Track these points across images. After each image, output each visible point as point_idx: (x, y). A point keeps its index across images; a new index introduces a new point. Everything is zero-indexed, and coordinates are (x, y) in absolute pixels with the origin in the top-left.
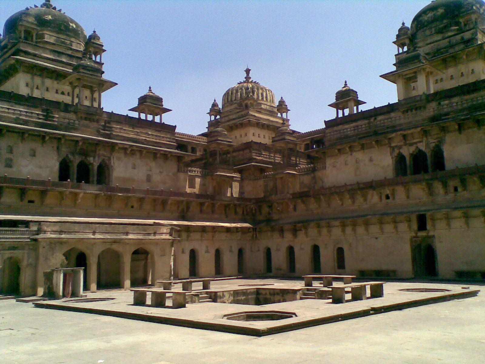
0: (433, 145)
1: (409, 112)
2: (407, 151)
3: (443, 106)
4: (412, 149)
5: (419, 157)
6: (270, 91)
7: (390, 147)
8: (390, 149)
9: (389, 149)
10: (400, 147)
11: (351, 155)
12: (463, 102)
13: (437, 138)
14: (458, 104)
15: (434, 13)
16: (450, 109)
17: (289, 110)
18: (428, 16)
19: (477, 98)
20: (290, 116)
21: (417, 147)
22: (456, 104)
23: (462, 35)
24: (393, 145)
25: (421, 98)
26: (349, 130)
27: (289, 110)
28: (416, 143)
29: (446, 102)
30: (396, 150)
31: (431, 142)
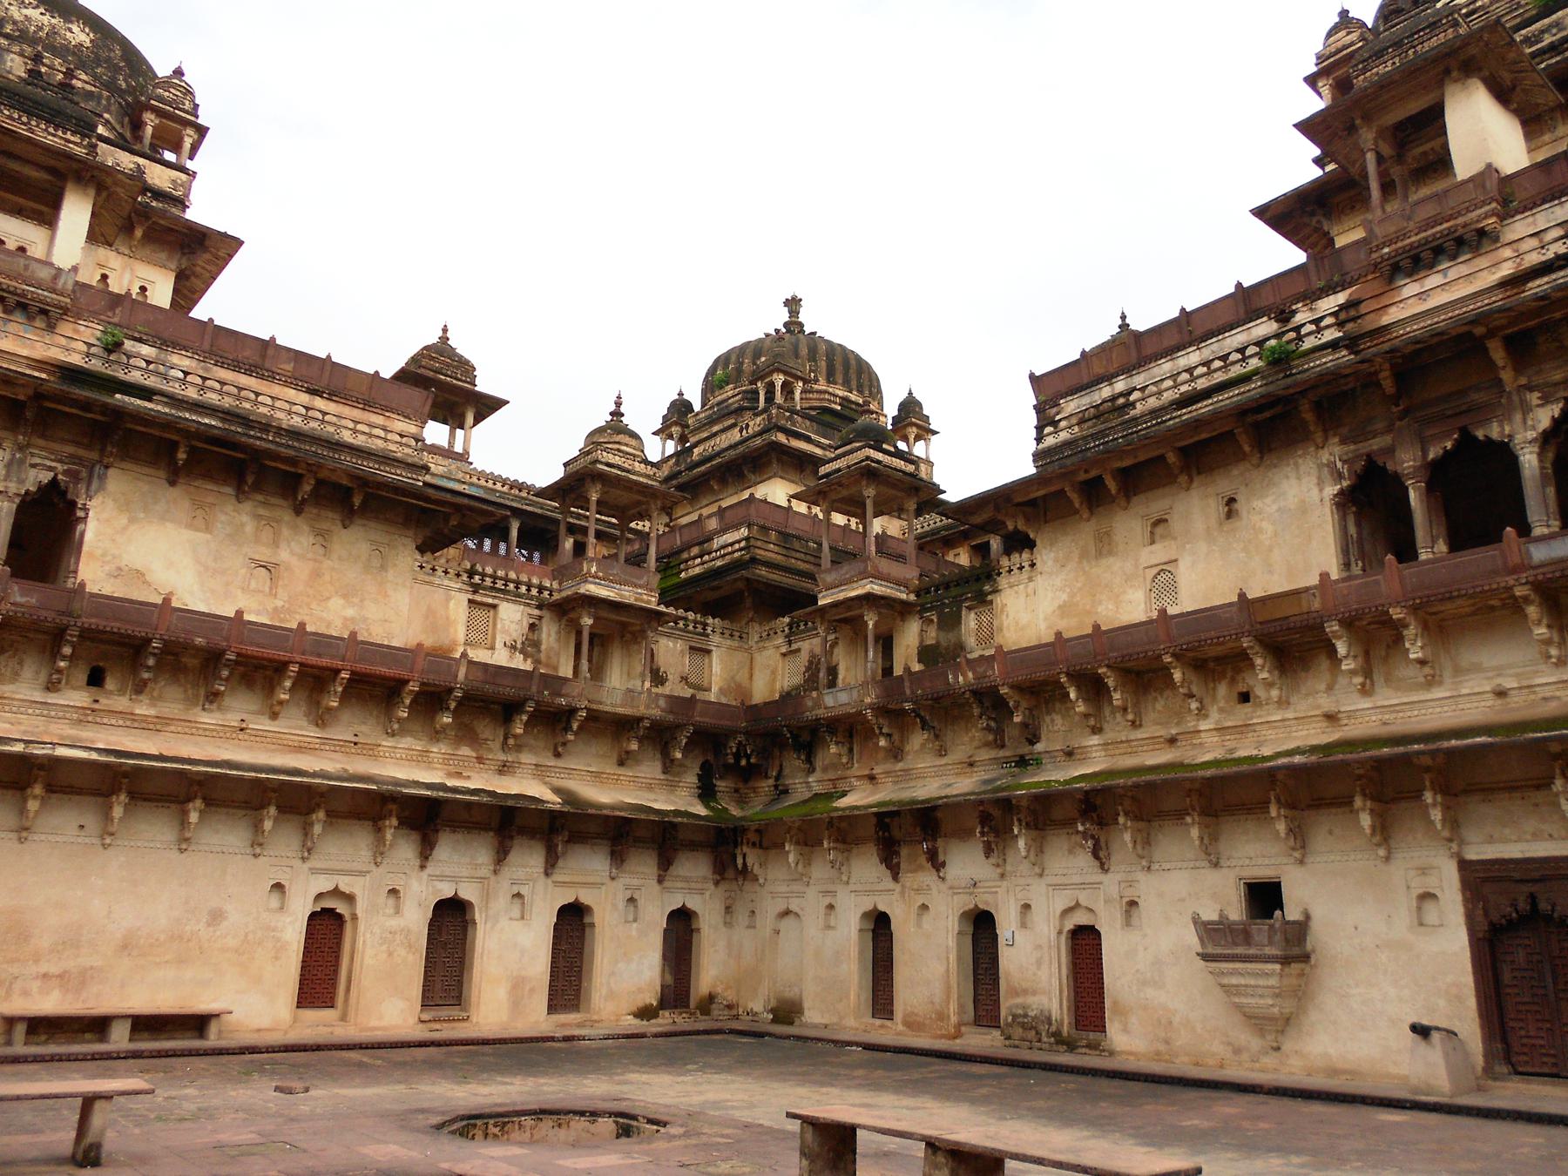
0: (46, 477)
3: (129, 357)
12: (209, 383)
14: (189, 378)
15: (53, 21)
16: (152, 382)
18: (25, 11)
22: (181, 375)
23: (141, 161)
25: (56, 278)
29: (146, 350)
31: (38, 461)
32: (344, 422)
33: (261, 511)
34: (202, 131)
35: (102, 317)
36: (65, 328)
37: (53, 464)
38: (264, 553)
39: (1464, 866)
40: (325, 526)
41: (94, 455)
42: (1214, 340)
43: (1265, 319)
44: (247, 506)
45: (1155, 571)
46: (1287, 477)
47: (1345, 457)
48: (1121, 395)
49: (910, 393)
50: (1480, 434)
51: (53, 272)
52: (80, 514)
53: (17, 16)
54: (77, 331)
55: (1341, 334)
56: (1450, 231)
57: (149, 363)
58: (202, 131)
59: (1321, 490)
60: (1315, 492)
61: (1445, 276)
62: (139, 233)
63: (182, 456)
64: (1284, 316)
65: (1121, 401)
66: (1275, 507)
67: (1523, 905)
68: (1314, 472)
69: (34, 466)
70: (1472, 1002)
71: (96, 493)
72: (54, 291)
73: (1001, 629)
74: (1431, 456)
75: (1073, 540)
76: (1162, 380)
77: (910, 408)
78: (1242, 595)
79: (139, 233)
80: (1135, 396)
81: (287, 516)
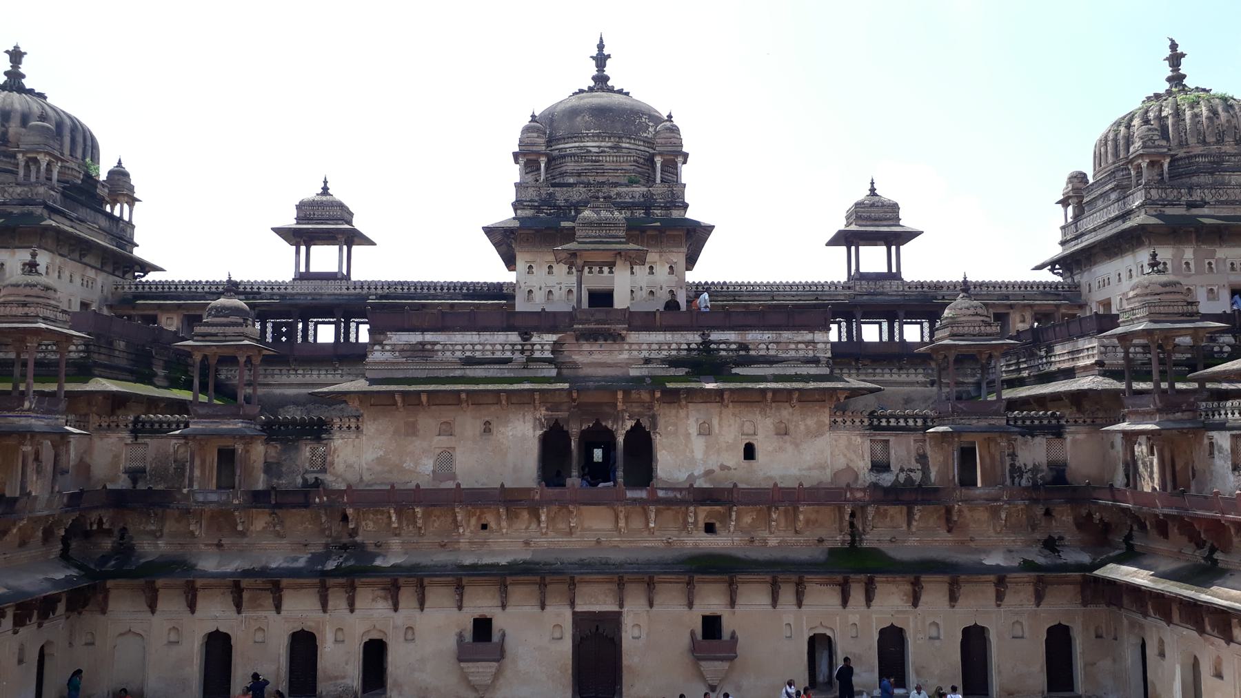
39: (575, 614)
42: (488, 333)
43: (517, 333)
45: (440, 451)
46: (518, 420)
47: (546, 417)
48: (429, 343)
49: (120, 163)
50: (604, 424)
55: (552, 356)
56: (609, 329)
59: (534, 431)
60: (531, 431)
61: (601, 346)
64: (526, 335)
65: (429, 347)
66: (511, 433)
67: (594, 630)
68: (532, 421)
70: (570, 671)
73: (332, 464)
74: (583, 428)
75: (389, 421)
76: (456, 344)
77: (119, 176)
78: (502, 485)
80: (438, 347)
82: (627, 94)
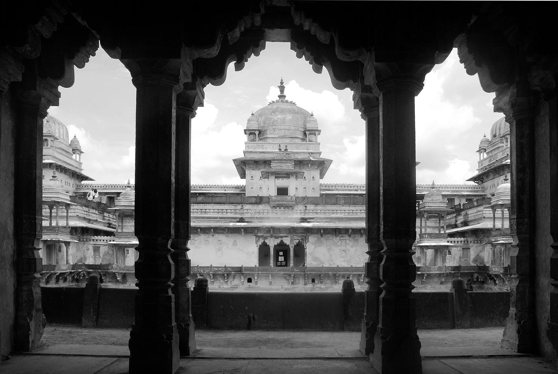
0: (297, 241)
1: (278, 208)
2: (272, 243)
4: (278, 241)
5: (282, 248)
6: (64, 127)
7: (256, 236)
8: (256, 238)
9: (255, 237)
10: (266, 238)
11: (213, 236)
13: (302, 236)
15: (283, 116)
17: (83, 153)
18: (277, 117)
19: (337, 211)
20: (83, 159)
21: (282, 241)
24: (259, 234)
26: (213, 211)
27: (83, 153)
28: (282, 237)
30: (261, 239)
31: (295, 238)
32: (358, 211)
33: (342, 238)
34: (319, 131)
35: (302, 203)
36: (296, 208)
37: (298, 238)
38: (344, 248)
40: (356, 238)
41: (306, 235)
44: (338, 238)
51: (291, 197)
52: (305, 247)
53: (276, 119)
54: (298, 208)
57: (313, 210)
58: (319, 131)
62: (310, 165)
63: (322, 231)
69: (295, 240)
71: (307, 242)
72: (291, 202)
79: (310, 165)
81: (347, 238)
82: (294, 104)
